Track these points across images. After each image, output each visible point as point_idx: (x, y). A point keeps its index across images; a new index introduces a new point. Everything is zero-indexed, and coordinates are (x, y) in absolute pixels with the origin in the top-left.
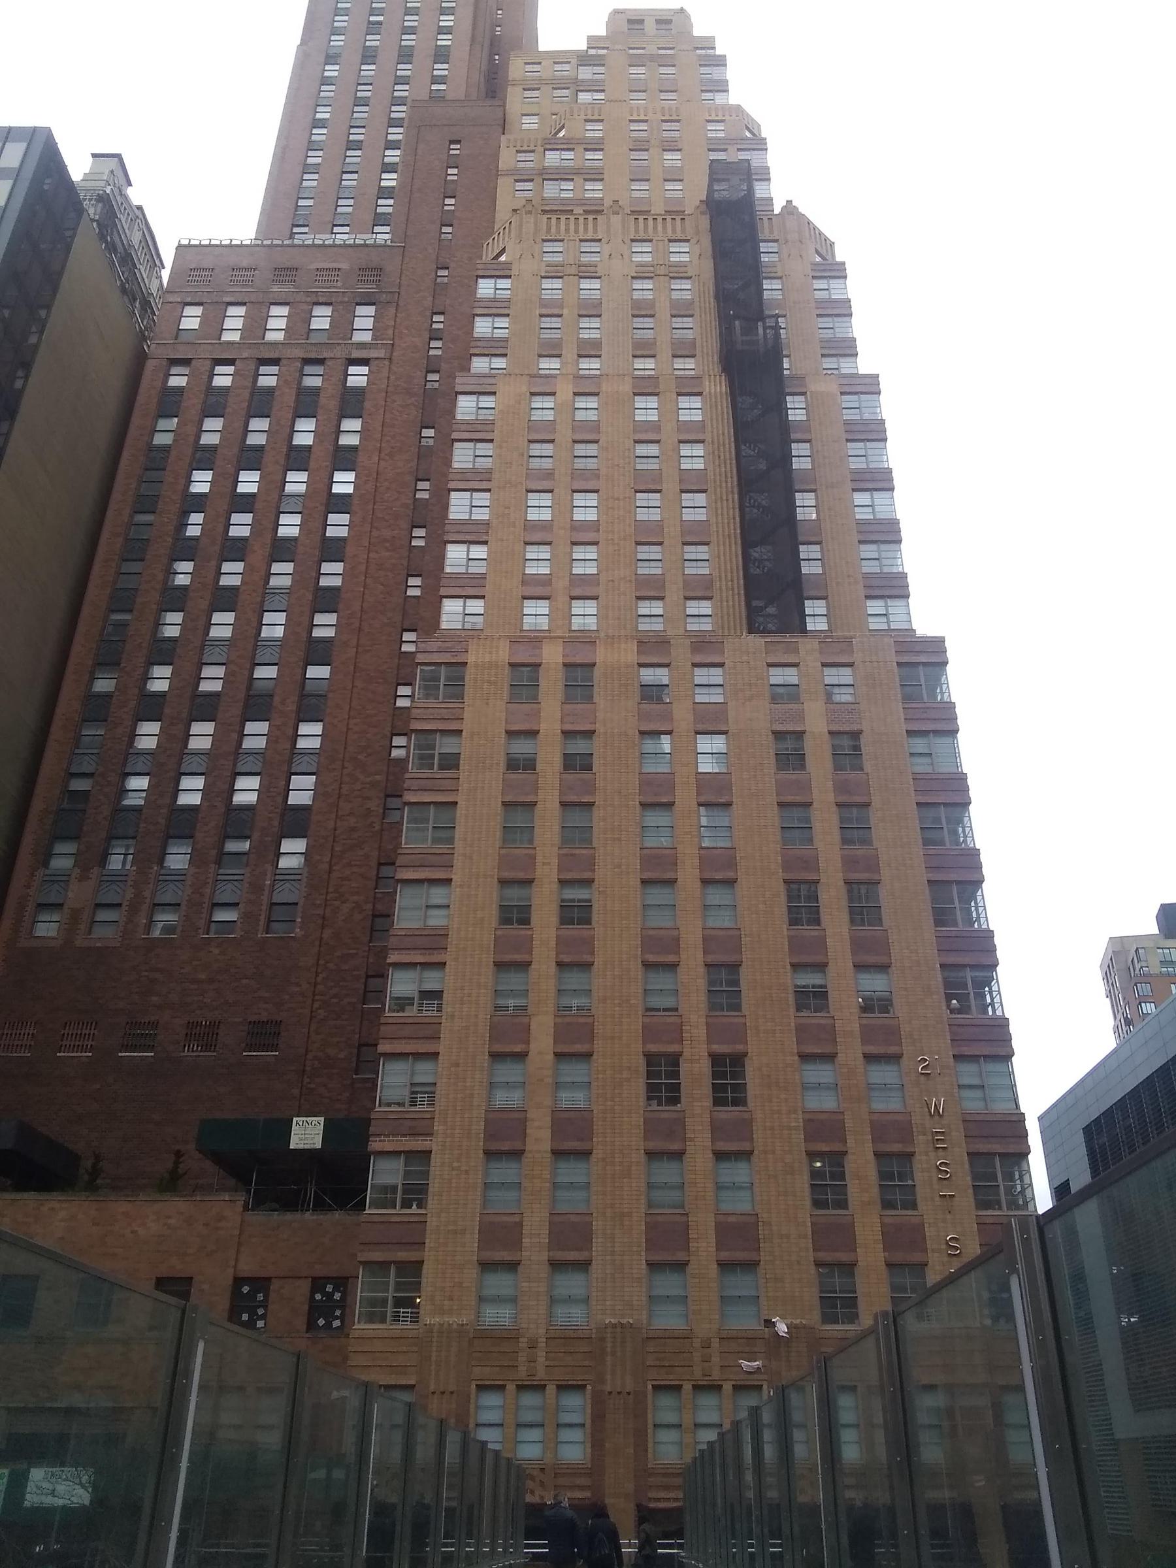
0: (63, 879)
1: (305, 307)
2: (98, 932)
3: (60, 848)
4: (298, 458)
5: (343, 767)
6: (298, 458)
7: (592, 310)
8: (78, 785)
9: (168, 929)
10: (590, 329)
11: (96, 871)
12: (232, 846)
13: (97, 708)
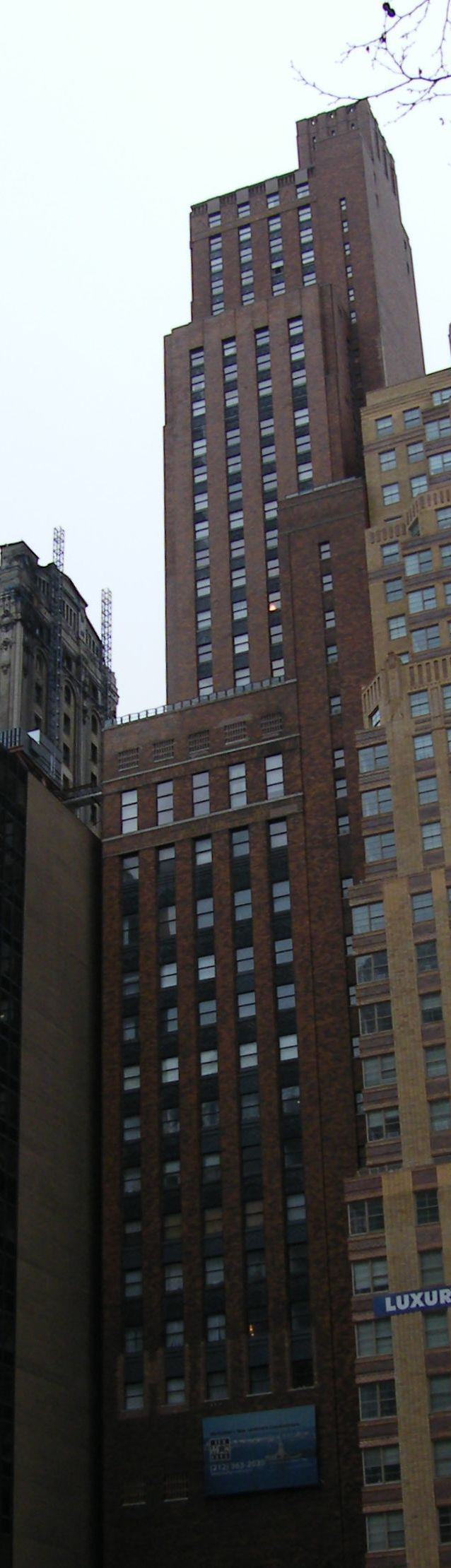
1: (221, 772)
4: (242, 934)
5: (327, 1234)
11: (160, 1351)
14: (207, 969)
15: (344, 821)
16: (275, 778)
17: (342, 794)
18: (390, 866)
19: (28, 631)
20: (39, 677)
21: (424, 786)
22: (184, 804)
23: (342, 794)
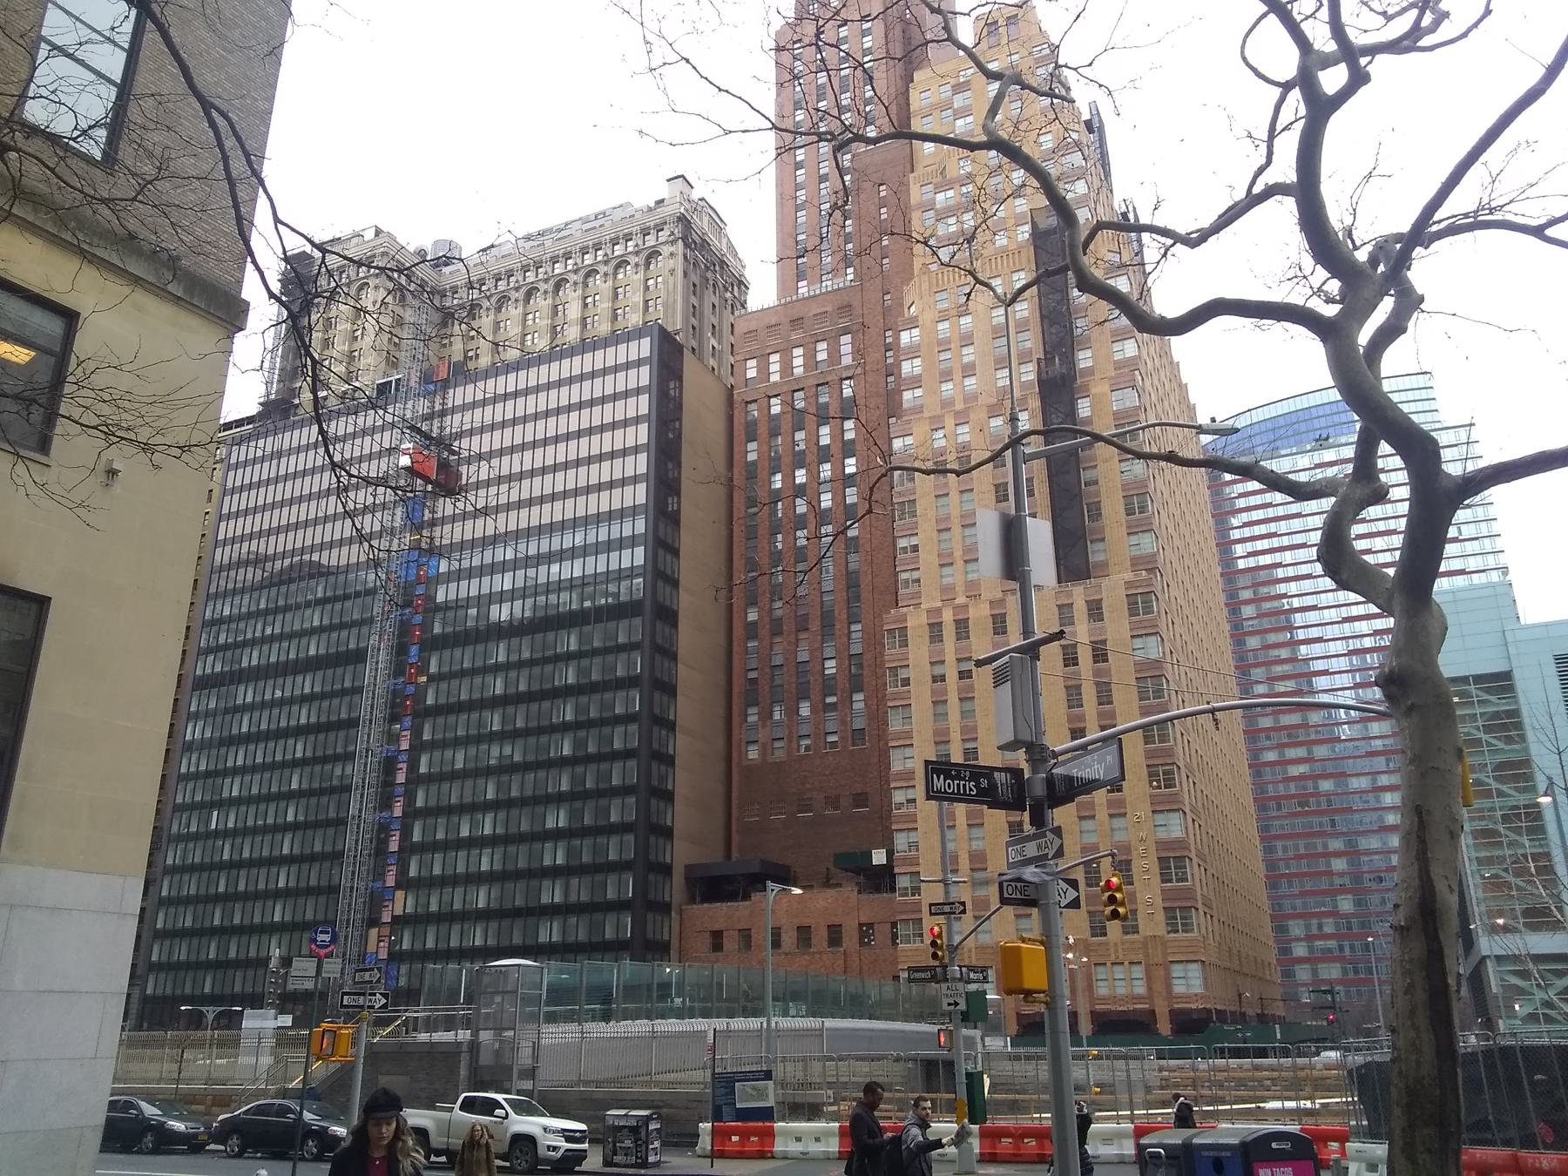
0: (754, 727)
2: (778, 753)
3: (750, 711)
4: (824, 455)
6: (824, 455)
7: (967, 340)
8: (752, 675)
9: (808, 748)
10: (969, 354)
12: (829, 700)
13: (752, 630)
14: (801, 476)
15: (890, 379)
16: (846, 349)
17: (889, 361)
18: (919, 410)
19: (686, 245)
20: (694, 278)
21: (943, 356)
22: (787, 367)
23: (889, 361)
